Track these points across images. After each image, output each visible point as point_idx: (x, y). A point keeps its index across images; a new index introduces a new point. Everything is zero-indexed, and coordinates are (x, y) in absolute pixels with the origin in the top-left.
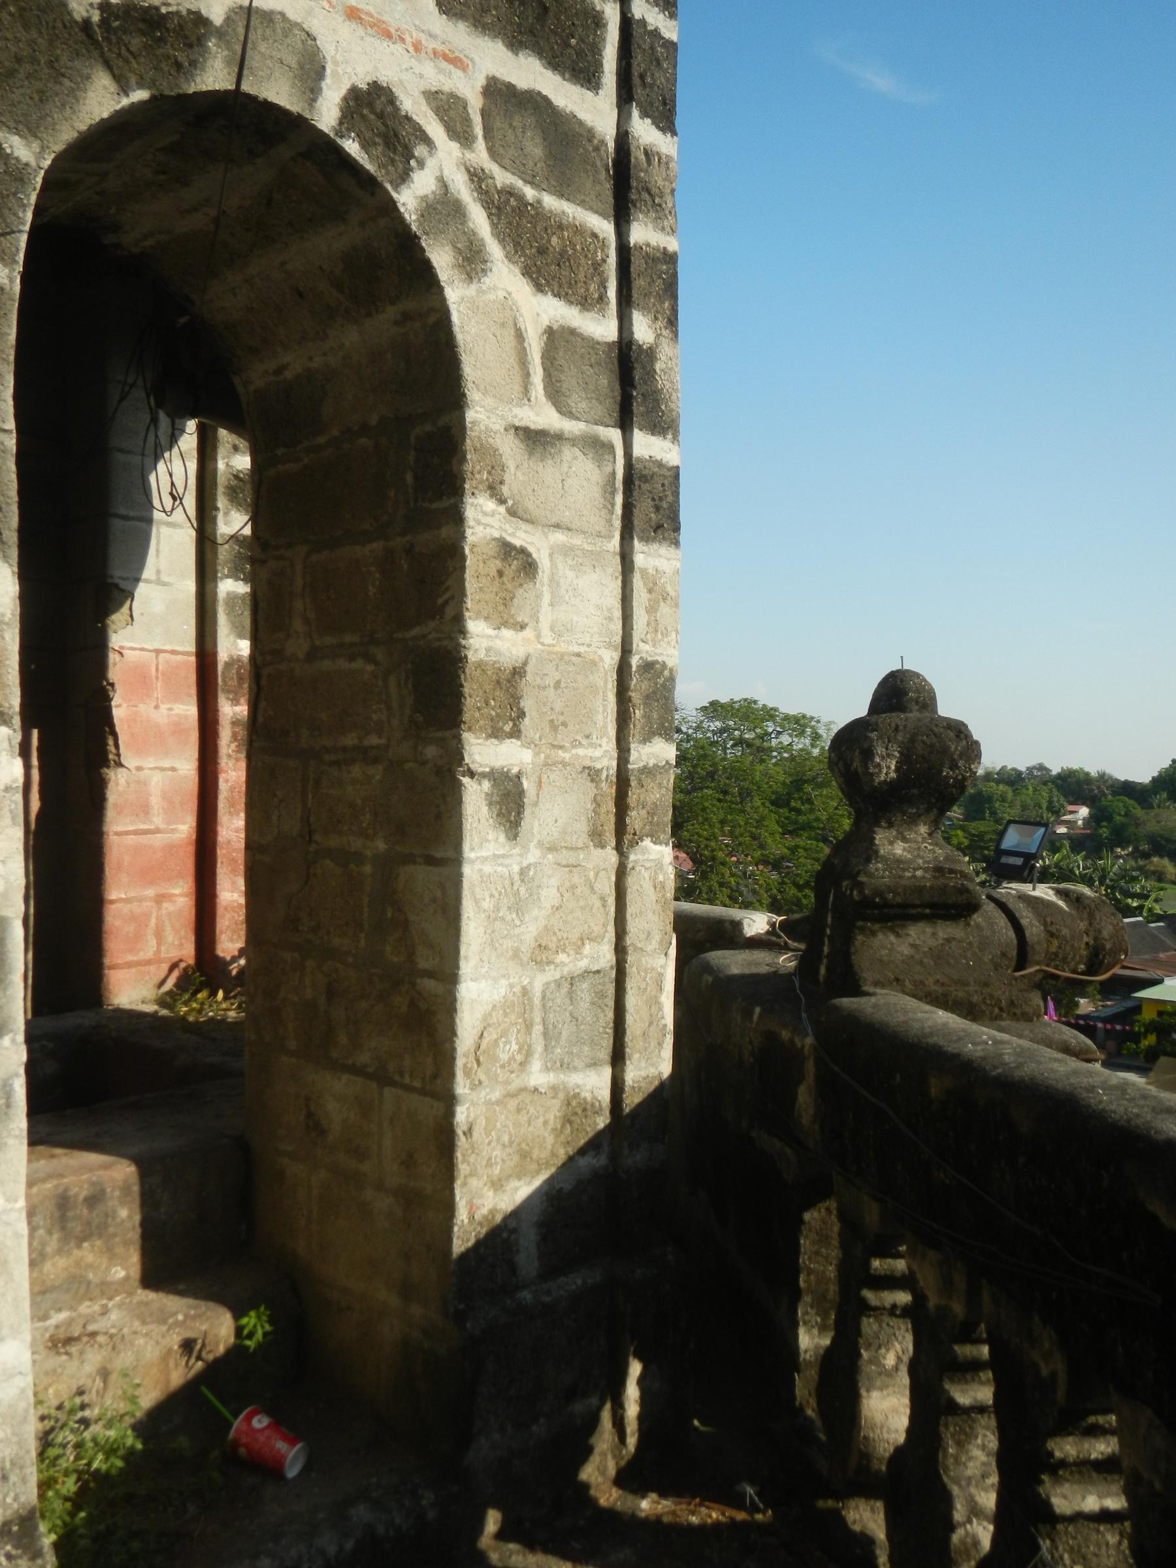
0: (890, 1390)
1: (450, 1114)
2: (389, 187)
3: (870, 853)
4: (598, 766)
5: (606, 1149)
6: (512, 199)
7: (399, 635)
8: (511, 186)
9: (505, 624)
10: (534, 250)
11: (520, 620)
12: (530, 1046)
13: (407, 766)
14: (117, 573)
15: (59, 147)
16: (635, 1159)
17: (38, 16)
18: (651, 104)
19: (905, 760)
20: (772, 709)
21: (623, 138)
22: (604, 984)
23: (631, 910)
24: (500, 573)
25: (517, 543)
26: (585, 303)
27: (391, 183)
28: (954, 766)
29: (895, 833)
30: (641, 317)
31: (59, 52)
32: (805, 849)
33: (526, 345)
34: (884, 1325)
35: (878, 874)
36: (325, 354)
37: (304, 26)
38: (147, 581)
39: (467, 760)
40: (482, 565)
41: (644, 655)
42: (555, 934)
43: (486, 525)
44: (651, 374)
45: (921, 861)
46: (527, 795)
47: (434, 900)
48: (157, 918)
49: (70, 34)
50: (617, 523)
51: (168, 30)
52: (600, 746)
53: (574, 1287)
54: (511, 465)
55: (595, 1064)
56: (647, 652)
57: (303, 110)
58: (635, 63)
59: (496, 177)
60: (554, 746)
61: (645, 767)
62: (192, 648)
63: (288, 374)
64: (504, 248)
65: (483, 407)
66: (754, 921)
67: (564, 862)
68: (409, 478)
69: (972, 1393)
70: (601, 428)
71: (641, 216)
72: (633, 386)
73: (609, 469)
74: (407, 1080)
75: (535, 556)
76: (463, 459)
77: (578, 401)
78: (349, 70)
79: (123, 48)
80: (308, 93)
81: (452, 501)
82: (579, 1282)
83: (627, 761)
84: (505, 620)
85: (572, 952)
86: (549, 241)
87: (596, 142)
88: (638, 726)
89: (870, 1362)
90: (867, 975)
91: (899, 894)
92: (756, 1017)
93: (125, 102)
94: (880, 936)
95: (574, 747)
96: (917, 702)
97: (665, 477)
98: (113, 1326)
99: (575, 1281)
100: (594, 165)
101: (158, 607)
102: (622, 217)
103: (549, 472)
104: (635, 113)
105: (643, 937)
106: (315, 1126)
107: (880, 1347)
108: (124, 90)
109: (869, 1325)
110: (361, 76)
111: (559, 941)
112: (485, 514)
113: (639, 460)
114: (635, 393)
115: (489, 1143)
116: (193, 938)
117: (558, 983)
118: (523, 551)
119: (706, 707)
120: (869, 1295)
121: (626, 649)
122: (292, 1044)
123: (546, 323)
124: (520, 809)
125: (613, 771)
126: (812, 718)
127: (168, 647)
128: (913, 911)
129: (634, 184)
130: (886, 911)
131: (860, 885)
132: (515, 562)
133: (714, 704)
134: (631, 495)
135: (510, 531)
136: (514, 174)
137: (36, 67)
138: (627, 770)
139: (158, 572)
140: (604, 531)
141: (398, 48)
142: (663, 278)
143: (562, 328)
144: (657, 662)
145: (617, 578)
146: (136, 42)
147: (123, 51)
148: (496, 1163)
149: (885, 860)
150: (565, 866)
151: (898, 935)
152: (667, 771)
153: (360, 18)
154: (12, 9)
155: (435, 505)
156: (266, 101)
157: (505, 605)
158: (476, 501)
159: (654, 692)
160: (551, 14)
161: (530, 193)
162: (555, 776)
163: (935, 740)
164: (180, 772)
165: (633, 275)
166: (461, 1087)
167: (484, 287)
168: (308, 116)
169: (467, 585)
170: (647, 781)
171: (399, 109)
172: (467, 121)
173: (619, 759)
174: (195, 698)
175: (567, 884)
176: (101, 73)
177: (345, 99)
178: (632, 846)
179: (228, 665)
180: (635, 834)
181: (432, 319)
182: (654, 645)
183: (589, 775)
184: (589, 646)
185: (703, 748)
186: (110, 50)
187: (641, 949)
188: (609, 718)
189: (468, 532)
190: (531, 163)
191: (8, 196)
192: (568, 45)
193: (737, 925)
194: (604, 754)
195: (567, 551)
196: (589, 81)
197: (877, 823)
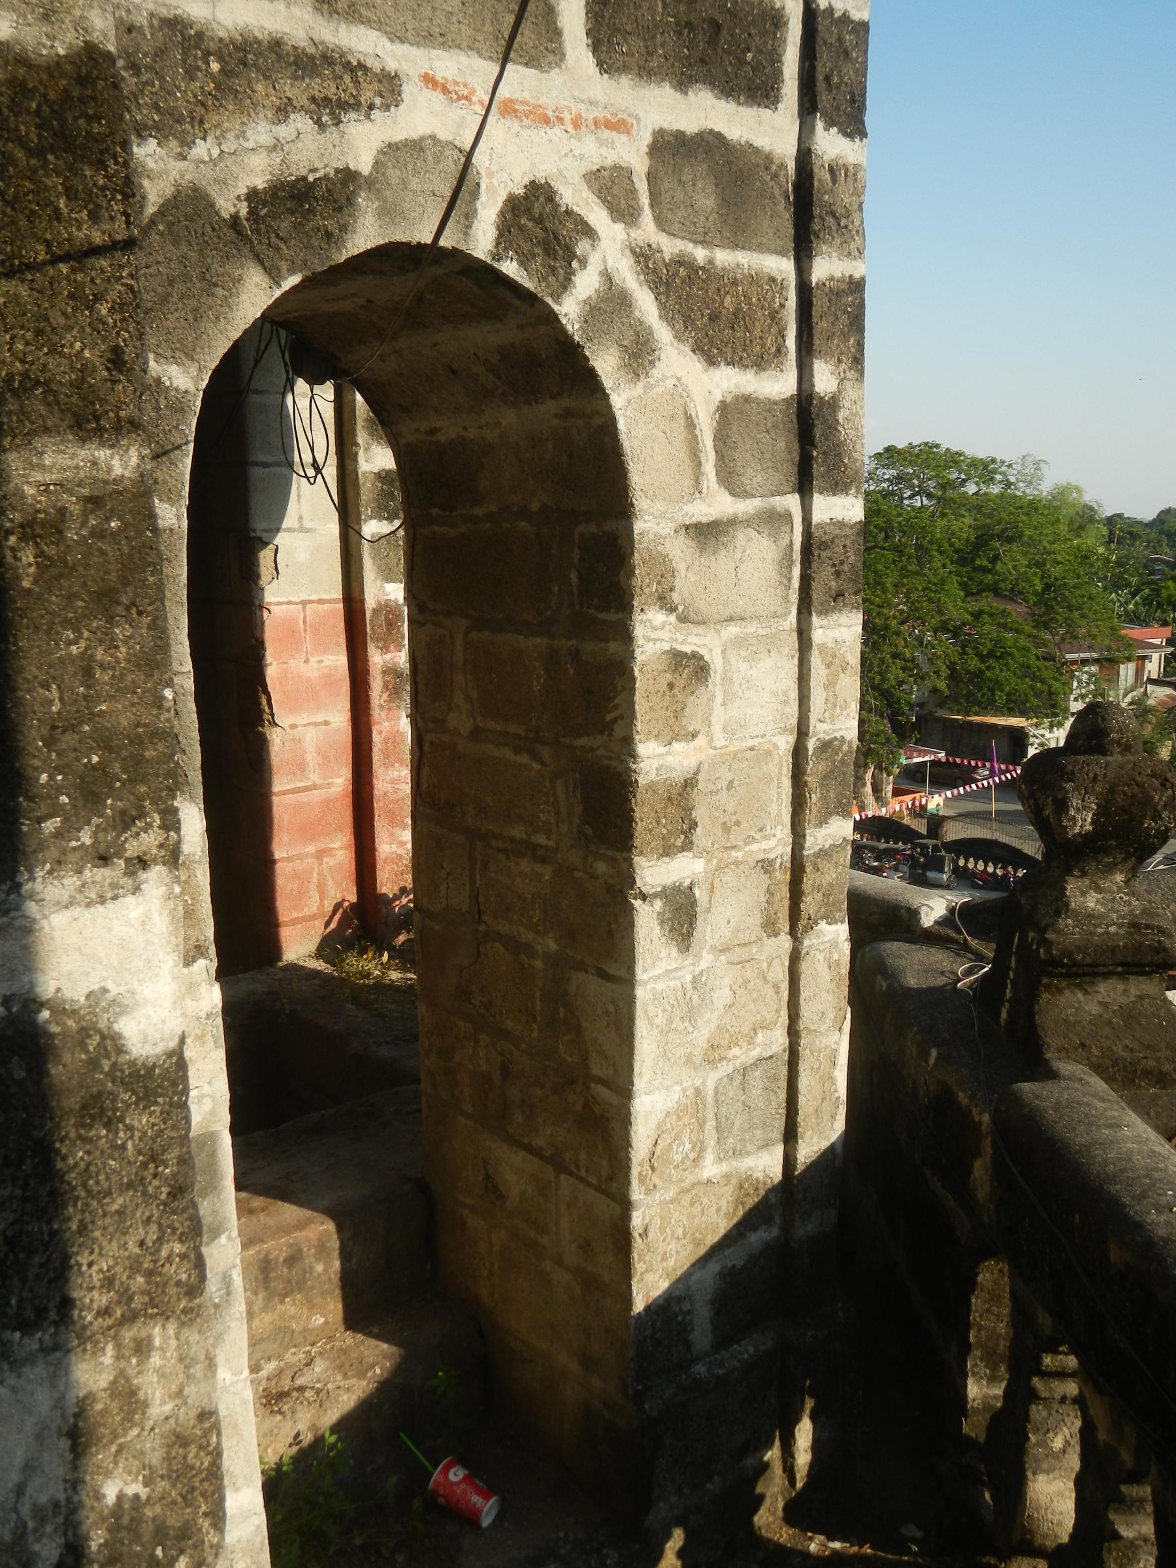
0: (1057, 1472)
1: (626, 1217)
2: (549, 300)
3: (1060, 906)
4: (772, 856)
5: (778, 1221)
6: (681, 269)
7: (566, 740)
8: (681, 254)
9: (676, 738)
10: (705, 319)
11: (691, 729)
12: (702, 1142)
13: (578, 874)
14: (259, 525)
15: (213, 365)
16: (807, 1228)
17: (187, 227)
18: (838, 108)
19: (1103, 812)
20: (957, 453)
21: (805, 156)
22: (777, 1068)
23: (804, 995)
24: (671, 686)
25: (688, 649)
26: (760, 363)
27: (552, 295)
28: (1156, 817)
29: (1088, 882)
30: (823, 365)
31: (209, 260)
32: (991, 615)
33: (697, 432)
34: (1053, 1412)
35: (1068, 931)
36: (481, 428)
37: (457, 143)
38: (289, 530)
39: (639, 883)
40: (652, 682)
41: (821, 736)
42: (727, 1031)
43: (655, 641)
44: (833, 426)
45: (1115, 916)
46: (699, 903)
47: (607, 1013)
48: (319, 874)
49: (219, 237)
50: (794, 597)
51: (316, 199)
52: (774, 836)
53: (746, 1356)
54: (681, 567)
55: (767, 1145)
56: (825, 732)
57: (458, 242)
58: (819, 65)
59: (665, 249)
60: (726, 848)
61: (821, 850)
62: (338, 594)
63: (441, 438)
64: (673, 327)
65: (652, 514)
66: (932, 909)
67: (737, 960)
68: (574, 576)
69: (1136, 1527)
70: (777, 498)
71: (824, 247)
72: (813, 445)
73: (786, 541)
74: (583, 1174)
75: (707, 658)
76: (631, 573)
77: (754, 477)
78: (505, 177)
79: (273, 235)
80: (463, 220)
81: (620, 616)
82: (751, 1349)
83: (802, 847)
84: (677, 732)
85: (744, 1044)
86: (722, 303)
87: (774, 167)
88: (814, 811)
89: (1038, 1444)
90: (1052, 1041)
91: (1089, 954)
92: (932, 1061)
93: (278, 293)
94: (1067, 993)
95: (747, 844)
96: (1119, 744)
97: (846, 536)
98: (318, 1381)
99: (746, 1349)
100: (772, 197)
101: (302, 556)
102: (803, 251)
103: (721, 563)
104: (820, 125)
105: (816, 1018)
106: (492, 1188)
107: (1048, 1431)
108: (277, 282)
109: (1037, 1412)
110: (517, 179)
111: (732, 1036)
112: (655, 628)
113: (820, 526)
114: (815, 454)
115: (664, 1240)
116: (355, 889)
117: (730, 1078)
118: (696, 656)
119: (879, 454)
120: (1036, 1382)
121: (802, 731)
122: (469, 1108)
123: (720, 398)
124: (692, 919)
125: (787, 858)
126: (1003, 462)
127: (315, 597)
128: (1103, 969)
129: (817, 211)
130: (1074, 969)
131: (1048, 944)
132: (686, 670)
133: (889, 450)
134: (810, 567)
135: (681, 638)
136: (683, 238)
137: (189, 285)
138: (802, 856)
139: (301, 518)
140: (780, 610)
141: (556, 132)
142: (848, 313)
143: (737, 398)
144: (836, 738)
145: (793, 657)
146: (285, 225)
147: (273, 239)
148: (671, 1256)
149: (1076, 915)
150: (740, 963)
151: (1086, 993)
152: (844, 848)
153: (515, 111)
154: (161, 227)
155: (602, 616)
156: (419, 243)
157: (676, 717)
158: (645, 617)
159: (832, 771)
160: (724, 32)
161: (700, 254)
162: (728, 877)
163: (1136, 790)
164: (333, 725)
165: (815, 320)
166: (637, 1193)
167: (652, 381)
168: (464, 248)
169: (637, 707)
170: (823, 864)
171: (559, 205)
172: (632, 192)
173: (794, 843)
174: (344, 646)
175: (740, 980)
176: (251, 264)
177: (502, 213)
178: (806, 932)
179: (375, 611)
180: (809, 919)
181: (597, 421)
182: (832, 722)
183: (763, 867)
184: (763, 736)
185: (876, 502)
186: (260, 242)
187: (815, 1031)
188: (784, 804)
189: (638, 652)
190: (702, 219)
191: (170, 431)
192: (742, 62)
193: (914, 914)
194: (778, 844)
195: (739, 642)
196: (767, 96)
197: (1069, 872)
